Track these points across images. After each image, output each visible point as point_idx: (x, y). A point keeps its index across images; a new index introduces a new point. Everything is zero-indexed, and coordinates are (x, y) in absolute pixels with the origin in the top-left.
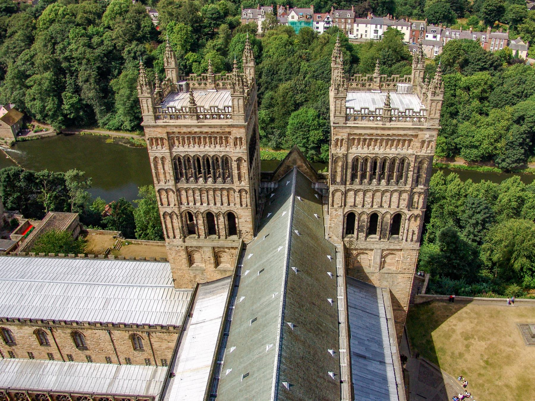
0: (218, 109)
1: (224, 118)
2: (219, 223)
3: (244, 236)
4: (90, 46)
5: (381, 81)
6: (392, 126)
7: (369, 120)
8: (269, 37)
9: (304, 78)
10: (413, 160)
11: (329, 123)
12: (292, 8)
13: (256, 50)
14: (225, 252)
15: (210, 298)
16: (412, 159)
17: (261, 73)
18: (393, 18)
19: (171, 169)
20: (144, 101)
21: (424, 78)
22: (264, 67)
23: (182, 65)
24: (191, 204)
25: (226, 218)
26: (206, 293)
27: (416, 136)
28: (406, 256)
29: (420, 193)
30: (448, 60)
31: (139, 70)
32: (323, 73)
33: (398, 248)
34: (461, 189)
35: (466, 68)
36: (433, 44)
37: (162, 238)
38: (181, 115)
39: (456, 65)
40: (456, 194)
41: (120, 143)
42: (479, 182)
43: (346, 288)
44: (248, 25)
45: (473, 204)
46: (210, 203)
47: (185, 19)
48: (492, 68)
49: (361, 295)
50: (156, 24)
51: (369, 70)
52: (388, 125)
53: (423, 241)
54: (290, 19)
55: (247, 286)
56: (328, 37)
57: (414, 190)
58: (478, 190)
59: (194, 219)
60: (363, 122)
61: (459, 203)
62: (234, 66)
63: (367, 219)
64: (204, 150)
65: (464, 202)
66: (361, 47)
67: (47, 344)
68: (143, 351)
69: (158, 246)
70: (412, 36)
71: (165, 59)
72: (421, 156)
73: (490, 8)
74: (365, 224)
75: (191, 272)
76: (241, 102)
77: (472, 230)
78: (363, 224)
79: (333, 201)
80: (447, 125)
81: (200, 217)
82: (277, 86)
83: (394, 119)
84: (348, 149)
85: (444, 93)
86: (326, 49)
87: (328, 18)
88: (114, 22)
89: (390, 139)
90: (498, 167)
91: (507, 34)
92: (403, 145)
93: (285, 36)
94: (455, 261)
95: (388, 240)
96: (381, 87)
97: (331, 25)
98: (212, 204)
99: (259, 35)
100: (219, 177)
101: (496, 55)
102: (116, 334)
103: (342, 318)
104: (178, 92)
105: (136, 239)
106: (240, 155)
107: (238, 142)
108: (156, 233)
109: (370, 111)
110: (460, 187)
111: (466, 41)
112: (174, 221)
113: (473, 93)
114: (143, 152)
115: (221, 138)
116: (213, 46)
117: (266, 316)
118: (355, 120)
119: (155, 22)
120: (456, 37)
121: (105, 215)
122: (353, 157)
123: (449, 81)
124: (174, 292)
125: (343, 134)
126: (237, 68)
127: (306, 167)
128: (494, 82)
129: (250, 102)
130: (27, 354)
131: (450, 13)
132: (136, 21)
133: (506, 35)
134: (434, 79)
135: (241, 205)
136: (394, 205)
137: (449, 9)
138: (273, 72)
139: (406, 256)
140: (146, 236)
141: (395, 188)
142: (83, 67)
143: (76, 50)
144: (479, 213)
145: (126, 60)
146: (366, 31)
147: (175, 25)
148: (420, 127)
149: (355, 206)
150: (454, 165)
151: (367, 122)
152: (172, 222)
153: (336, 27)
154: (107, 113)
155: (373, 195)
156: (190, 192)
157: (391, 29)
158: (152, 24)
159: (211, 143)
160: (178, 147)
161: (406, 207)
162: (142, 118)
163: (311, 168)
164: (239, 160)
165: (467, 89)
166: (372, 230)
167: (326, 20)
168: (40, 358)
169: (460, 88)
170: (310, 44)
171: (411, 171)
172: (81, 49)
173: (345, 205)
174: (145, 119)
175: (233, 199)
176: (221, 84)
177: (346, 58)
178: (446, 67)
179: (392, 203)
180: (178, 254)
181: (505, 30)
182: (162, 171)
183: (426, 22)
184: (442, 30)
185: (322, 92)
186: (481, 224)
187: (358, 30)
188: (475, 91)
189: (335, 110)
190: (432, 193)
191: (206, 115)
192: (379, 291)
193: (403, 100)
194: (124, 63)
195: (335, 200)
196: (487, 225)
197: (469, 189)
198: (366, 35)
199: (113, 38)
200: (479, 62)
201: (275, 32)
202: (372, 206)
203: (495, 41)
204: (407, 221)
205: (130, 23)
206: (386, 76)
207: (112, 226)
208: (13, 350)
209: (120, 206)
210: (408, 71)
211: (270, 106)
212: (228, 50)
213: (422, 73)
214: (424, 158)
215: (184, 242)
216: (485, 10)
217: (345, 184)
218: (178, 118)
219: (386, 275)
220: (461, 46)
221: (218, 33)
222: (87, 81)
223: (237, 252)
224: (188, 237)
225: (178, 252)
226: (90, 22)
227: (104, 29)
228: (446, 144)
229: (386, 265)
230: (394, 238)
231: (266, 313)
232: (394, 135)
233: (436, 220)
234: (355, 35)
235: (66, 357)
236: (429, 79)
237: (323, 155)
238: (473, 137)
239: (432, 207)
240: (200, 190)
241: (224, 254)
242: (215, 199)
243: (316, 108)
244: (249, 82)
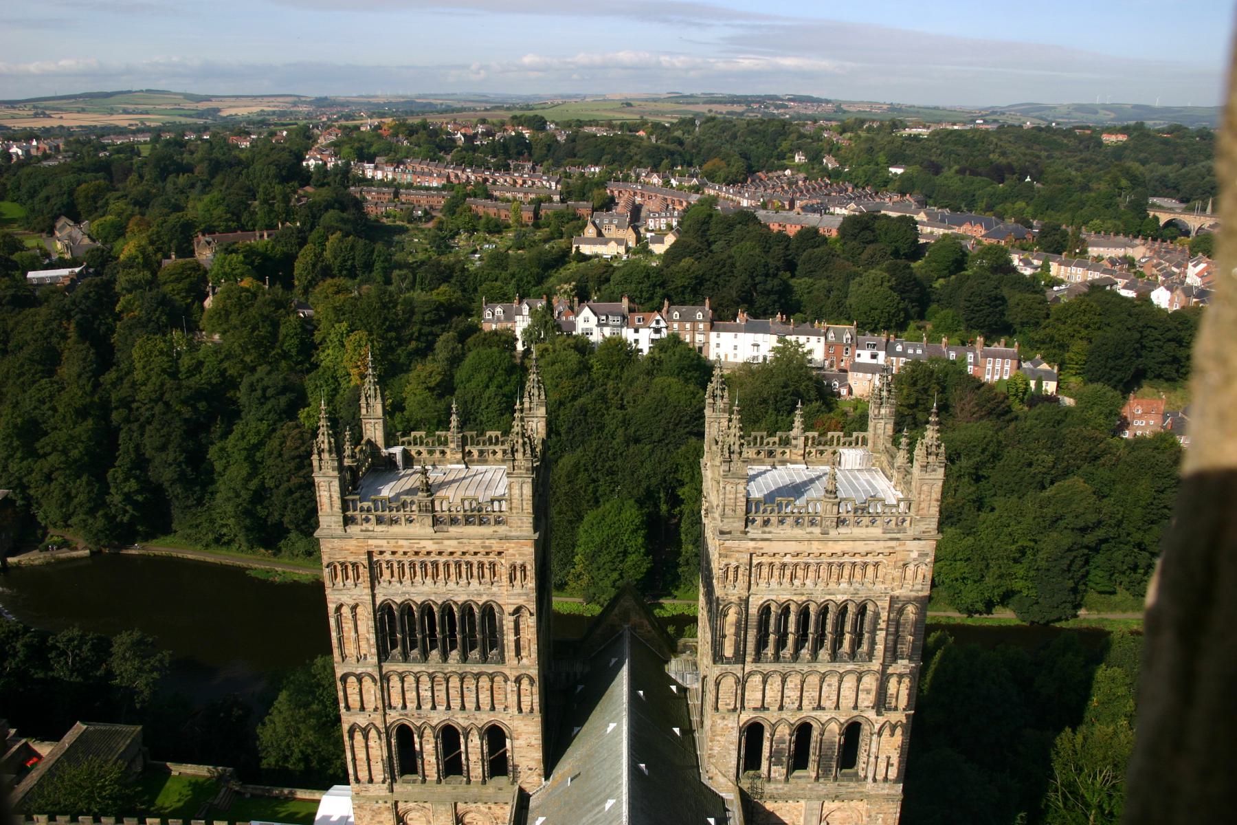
2: (469, 750)
10: (887, 605)
24: (411, 706)
29: (901, 676)
63: (791, 735)
78: (781, 746)
106: (521, 601)
112: (371, 743)
135: (520, 710)
139: (873, 814)
148: (898, 536)
149: (763, 708)
152: (367, 747)
156: (410, 680)
164: (518, 611)
166: (799, 759)
173: (743, 707)
175: (502, 697)
180: (377, 819)
182: (353, 634)
202: (800, 708)
204: (875, 737)
215: (392, 791)
225: (376, 813)
240: (432, 678)
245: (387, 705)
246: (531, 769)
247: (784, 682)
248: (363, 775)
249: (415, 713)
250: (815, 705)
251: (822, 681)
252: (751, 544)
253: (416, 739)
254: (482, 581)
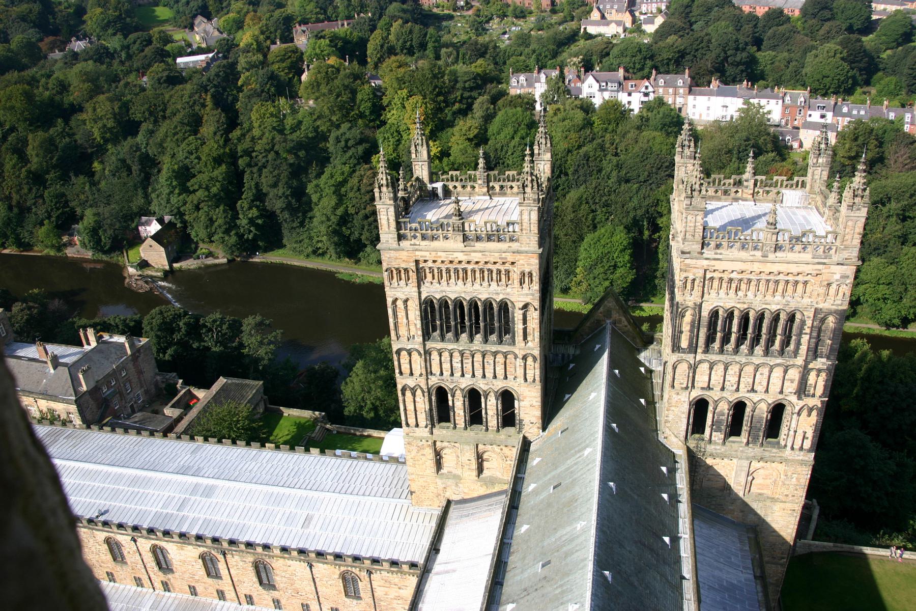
2: (488, 407)
10: (812, 315)
16: (810, 314)
24: (447, 373)
29: (819, 371)
63: (729, 410)
67: (218, 576)
68: (359, 598)
74: (724, 418)
78: (721, 417)
102: (320, 568)
106: (528, 299)
112: (417, 399)
114: (376, 292)
130: (188, 588)
135: (526, 380)
139: (789, 474)
149: (709, 388)
156: (446, 355)
159: (483, 280)
164: (525, 307)
166: (735, 428)
168: (206, 596)
173: (693, 386)
175: (512, 370)
182: (405, 320)
202: (737, 390)
204: (795, 416)
208: (169, 579)
217: (696, 353)
225: (420, 448)
235: (243, 598)
245: (429, 372)
246: (532, 423)
247: (726, 369)
248: (412, 421)
249: (449, 378)
250: (750, 389)
251: (756, 370)
252: (706, 263)
253: (450, 398)
254: (500, 284)
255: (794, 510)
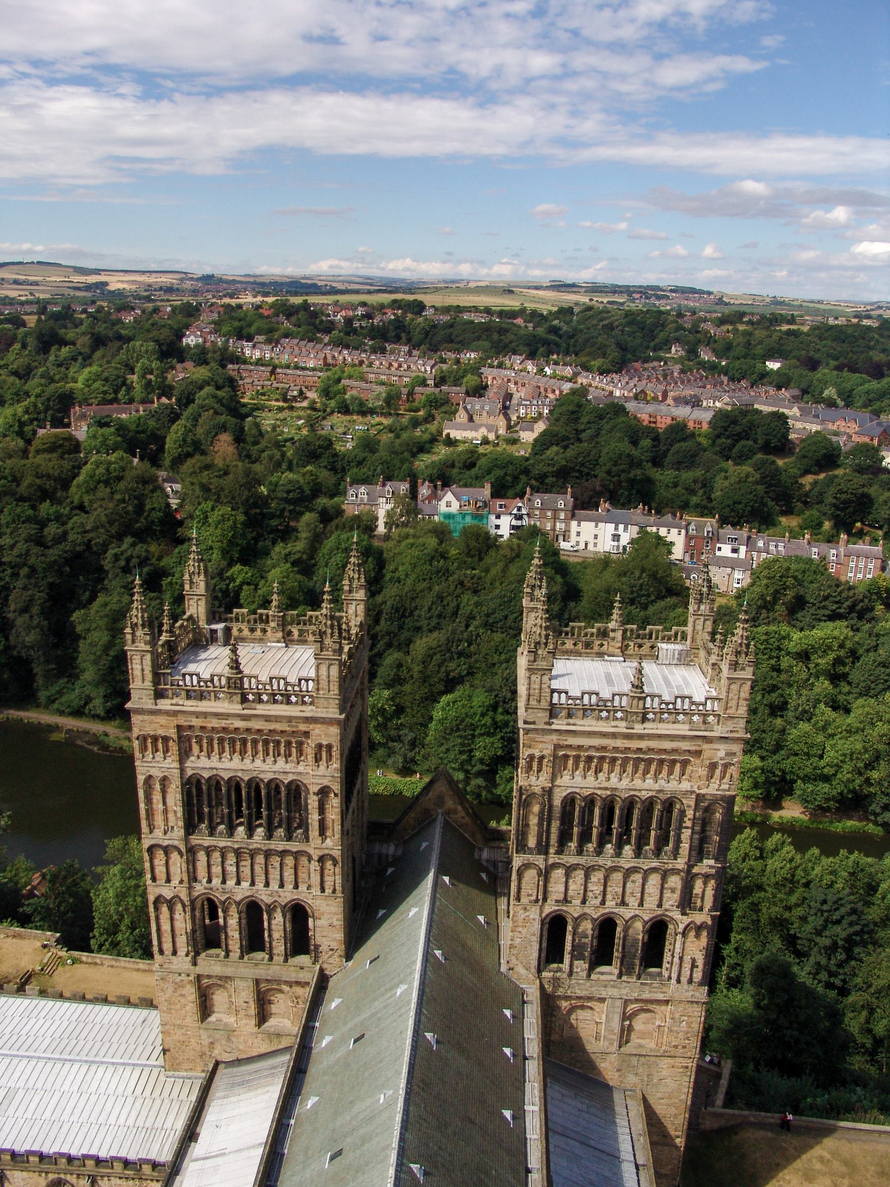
0: (287, 684)
1: (297, 703)
2: (273, 927)
3: (324, 957)
4: (39, 541)
5: (624, 638)
6: (646, 731)
7: (600, 718)
8: (399, 542)
9: (467, 626)
10: (692, 803)
11: (516, 721)
12: (449, 486)
13: (372, 566)
14: (281, 991)
15: (241, 1097)
17: (380, 613)
18: (650, 511)
19: (180, 803)
20: (136, 659)
21: (713, 634)
22: (385, 602)
23: (221, 589)
24: (216, 882)
25: (288, 916)
26: (233, 1085)
27: (698, 753)
28: (677, 1016)
29: (707, 877)
30: (762, 597)
31: (132, 595)
32: (506, 617)
33: (660, 997)
34: (796, 868)
35: (799, 615)
36: (733, 565)
37: (148, 954)
38: (209, 692)
39: (780, 609)
40: (785, 879)
41: (79, 742)
42: (835, 854)
43: (545, 1086)
44: (358, 516)
45: (824, 902)
46: (257, 880)
47: (233, 498)
48: (854, 615)
49: (579, 1106)
50: (175, 507)
51: (600, 615)
52: (638, 729)
53: (717, 983)
54: (442, 507)
55: (325, 1074)
56: (519, 547)
57: (695, 870)
58: (833, 872)
59: (221, 914)
60: (586, 722)
61: (793, 899)
62: (325, 597)
63: (593, 930)
64: (251, 767)
65: (805, 899)
66: (585, 568)
69: (138, 970)
70: (688, 548)
71: (187, 577)
72: (708, 797)
73: (843, 496)
74: (587, 940)
75: (204, 1035)
76: (335, 671)
77: (824, 962)
78: (583, 940)
79: (519, 889)
80: (764, 731)
81: (233, 911)
82: (409, 642)
83: (651, 716)
84: (553, 779)
85: (756, 664)
86: (513, 570)
87: (519, 509)
88: (92, 497)
89: (643, 760)
90: (876, 823)
91: (880, 548)
92: (670, 773)
93: (432, 542)
94: (789, 1032)
95: (639, 978)
96: (624, 649)
97: (525, 522)
98: (260, 885)
99: (379, 537)
100: (280, 826)
101: (861, 589)
103: (535, 1158)
104: (207, 645)
105: (92, 952)
106: (326, 782)
107: (324, 754)
108: (135, 942)
109: (600, 699)
110: (793, 864)
111: (799, 559)
112: (177, 916)
113: (817, 665)
115: (288, 744)
116: (286, 555)
117: (362, 1145)
118: (569, 716)
119: (174, 502)
120: (778, 551)
121: (31, 895)
122: (564, 794)
123: (766, 640)
124: (162, 1078)
125: (543, 747)
126: (331, 601)
127: (463, 814)
128: (858, 643)
129: (354, 671)
131: (765, 505)
132: (136, 498)
133: (878, 549)
134: (733, 635)
135: (323, 890)
136: (651, 902)
137: (762, 498)
138: (402, 613)
139: (677, 1016)
140: (115, 949)
141: (654, 865)
142: (19, 584)
143: (12, 547)
144: (838, 922)
145: (107, 572)
146: (596, 537)
147: (213, 509)
149: (566, 900)
150: (781, 817)
151: (594, 722)
152: (172, 919)
153: (535, 525)
154: (59, 678)
155: (606, 878)
156: (216, 855)
157: (647, 532)
158: (168, 505)
159: (268, 754)
160: (198, 757)
161: (678, 907)
162: (129, 693)
163: (475, 816)
164: (324, 792)
165: (804, 656)
167: (515, 511)
169: (788, 654)
170: (481, 559)
171: (687, 828)
172: (21, 547)
173: (545, 899)
174: (134, 695)
175: (305, 876)
176: (296, 633)
177: (554, 589)
178: (758, 612)
179: (646, 897)
180: (179, 992)
181: (877, 540)
182: (161, 806)
183: (717, 522)
184: (749, 538)
185: (503, 657)
186: (843, 947)
187: (578, 534)
188: (820, 661)
189: (529, 695)
190: (733, 877)
191: (260, 695)
192: (618, 1097)
193: (670, 677)
194: (104, 579)
195: (523, 886)
196: (857, 950)
197: (813, 869)
198: (595, 545)
199: (88, 528)
200: (826, 603)
201: (411, 531)
202: (603, 902)
203: (857, 561)
204: (679, 937)
205: (123, 501)
206: (635, 627)
207: (42, 919)
209: (65, 878)
210: (682, 619)
211: (396, 681)
212: (315, 565)
213: (709, 624)
214: (715, 800)
215: (195, 964)
216: (834, 501)
217: (546, 853)
218: (201, 696)
219: (634, 1060)
220: (788, 569)
221: (296, 530)
222: (25, 610)
223: (306, 993)
224: (203, 955)
225: (179, 986)
226: (45, 495)
227: (72, 509)
228: (763, 772)
229: (633, 1036)
230: (652, 976)
231: (364, 1140)
232: (650, 750)
233: (742, 936)
234: (573, 543)
236: (725, 635)
237: (501, 787)
238: (821, 757)
239: (734, 906)
240: (238, 853)
241: (279, 995)
242: (267, 873)
243: (490, 690)
244: (353, 631)
246: (332, 950)
250: (619, 901)
255: (687, 1067)
